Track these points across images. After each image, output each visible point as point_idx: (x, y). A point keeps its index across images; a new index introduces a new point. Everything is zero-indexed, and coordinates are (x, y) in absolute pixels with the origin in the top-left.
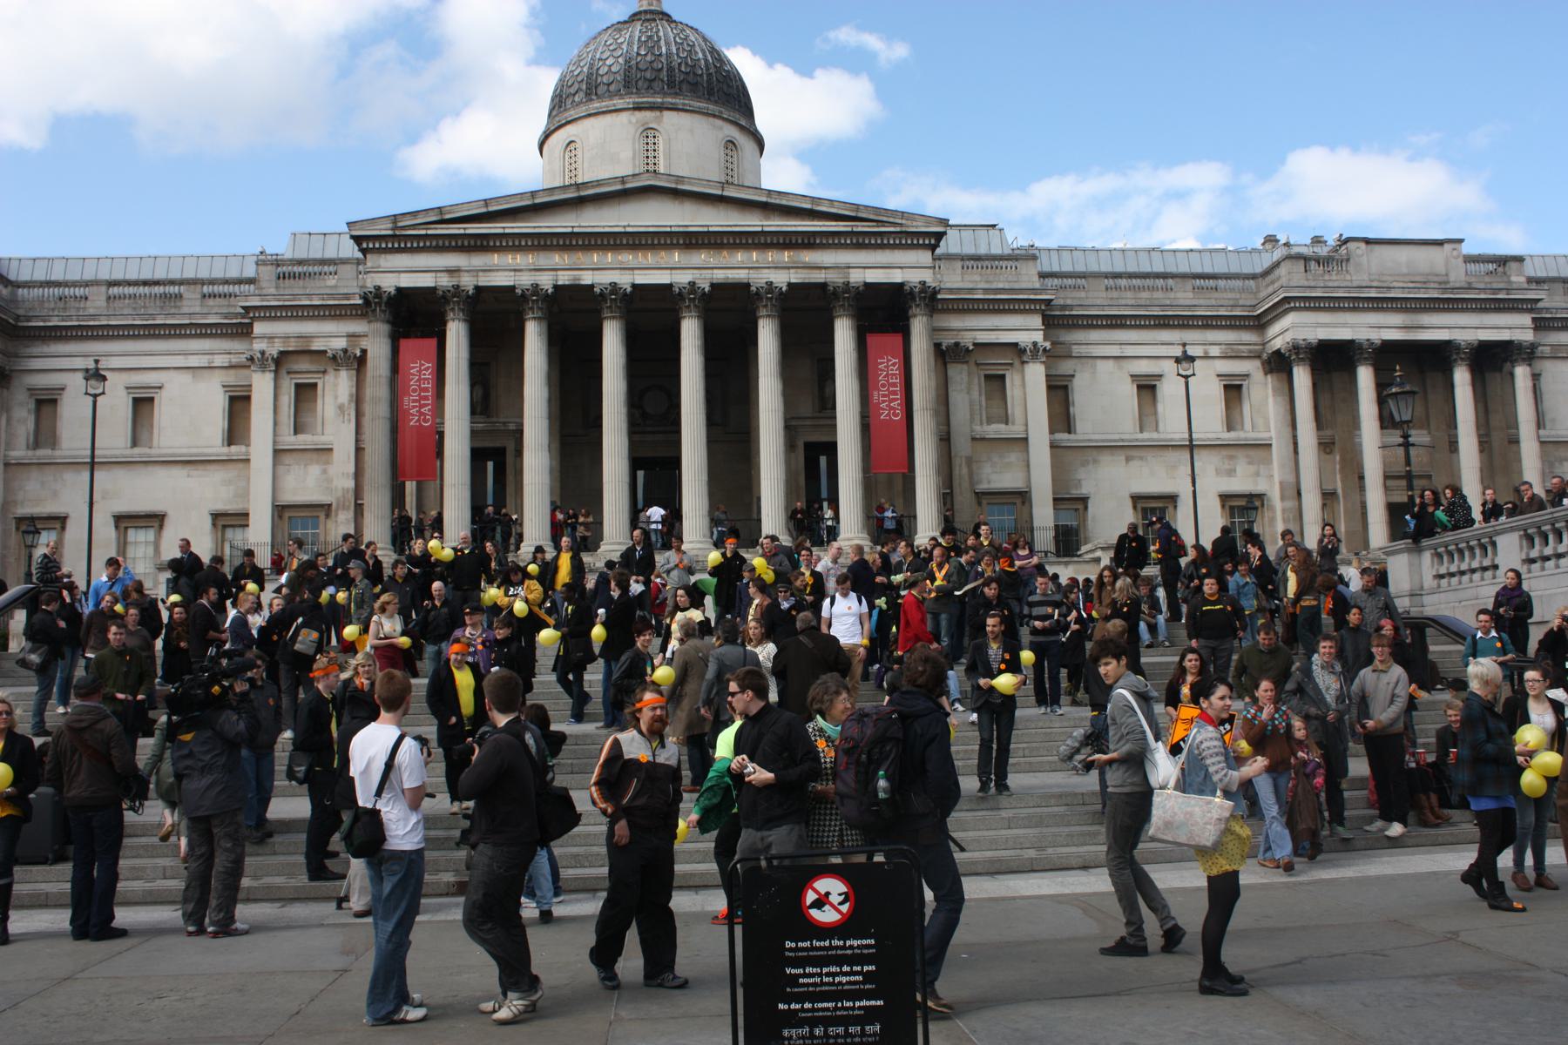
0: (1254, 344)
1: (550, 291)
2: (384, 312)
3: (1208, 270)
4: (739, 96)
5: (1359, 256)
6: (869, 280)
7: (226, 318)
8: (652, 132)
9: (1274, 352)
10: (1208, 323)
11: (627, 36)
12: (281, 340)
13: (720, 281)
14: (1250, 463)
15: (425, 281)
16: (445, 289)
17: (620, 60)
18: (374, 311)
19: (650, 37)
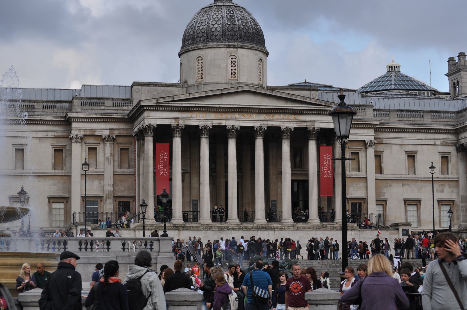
0: (453, 140)
2: (151, 133)
3: (437, 109)
6: (321, 127)
8: (233, 56)
10: (436, 131)
11: (222, 14)
12: (83, 130)
13: (270, 126)
14: (449, 188)
15: (166, 122)
16: (174, 126)
17: (220, 26)
18: (149, 132)
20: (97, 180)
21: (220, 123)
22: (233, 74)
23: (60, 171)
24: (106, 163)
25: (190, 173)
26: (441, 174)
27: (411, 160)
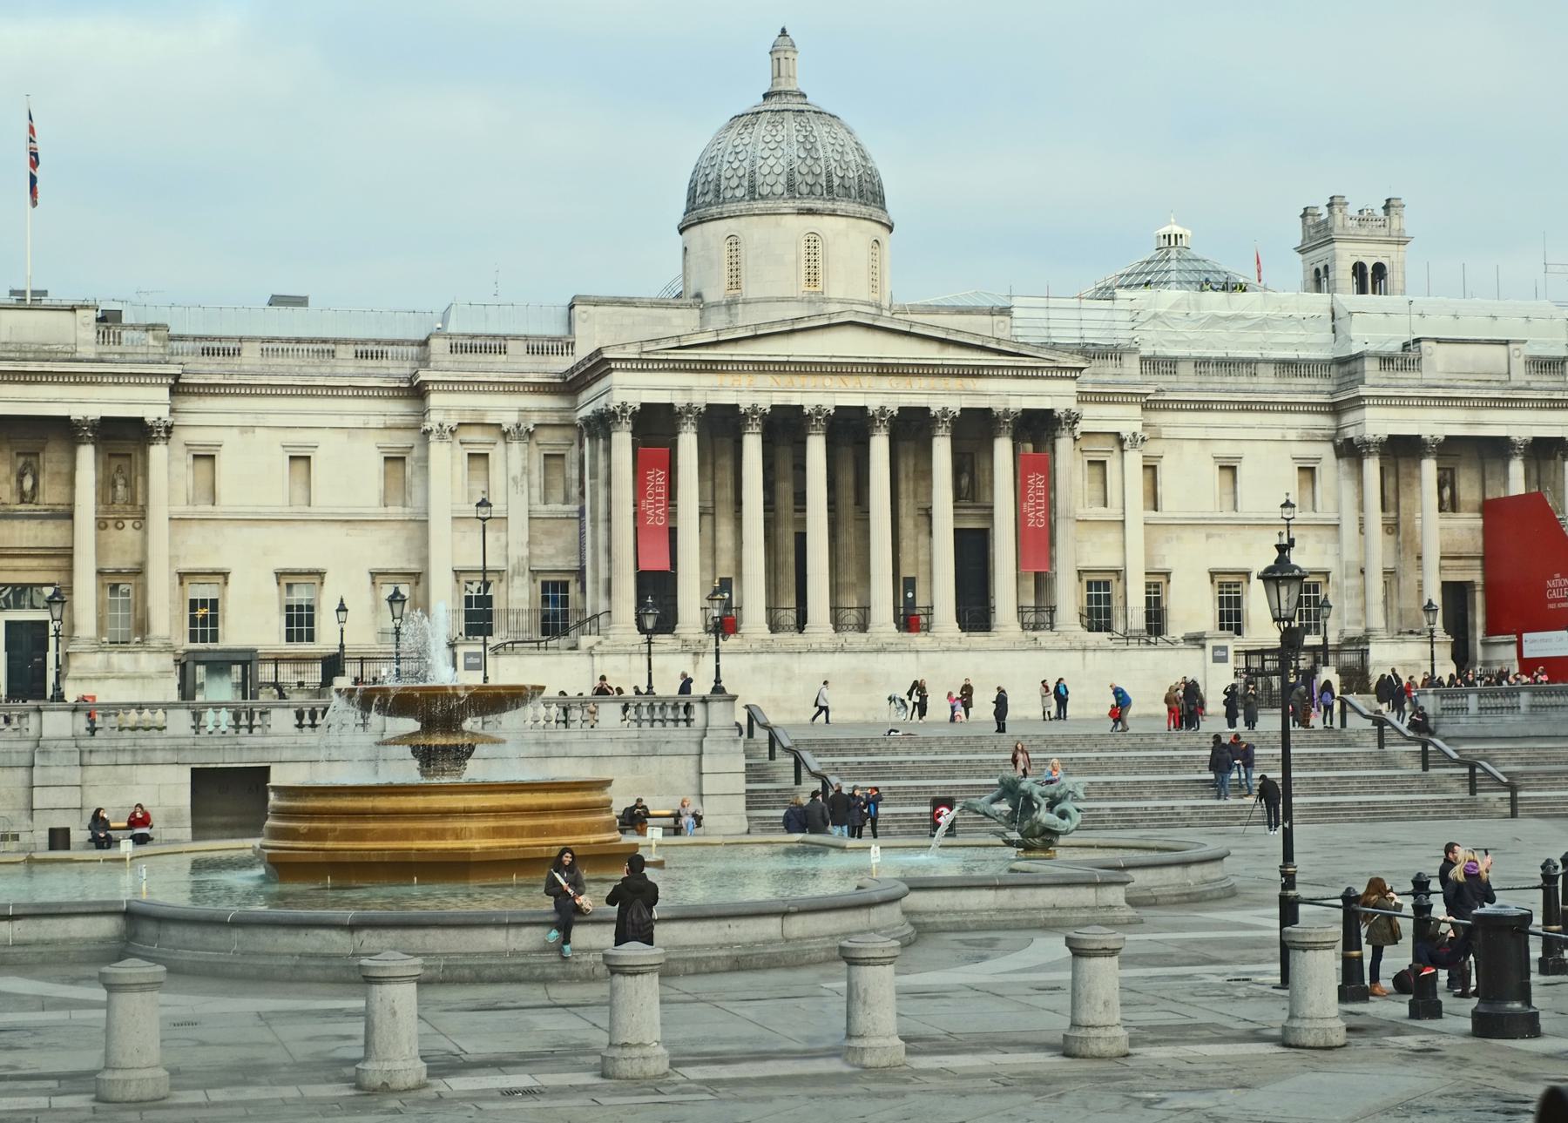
5: (1430, 355)
7: (385, 382)
9: (1345, 439)
10: (1287, 408)
11: (785, 132)
14: (1319, 542)
17: (781, 161)
19: (805, 137)
22: (812, 279)
23: (400, 509)
24: (512, 490)
25: (713, 514)
27: (1227, 475)
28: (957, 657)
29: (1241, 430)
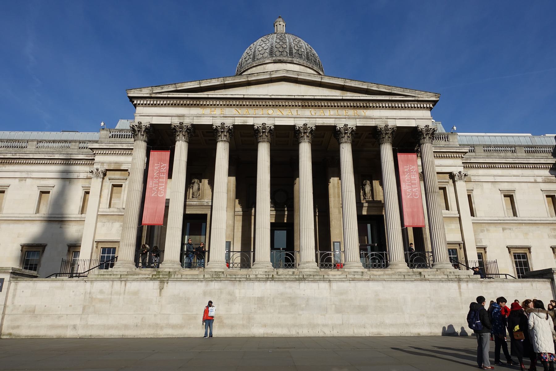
1: (230, 127)
4: (319, 64)
6: (398, 125)
10: (535, 166)
12: (107, 164)
13: (319, 125)
16: (175, 125)
20: (118, 221)
21: (245, 121)
26: (549, 216)
28: (360, 285)
29: (512, 177)
